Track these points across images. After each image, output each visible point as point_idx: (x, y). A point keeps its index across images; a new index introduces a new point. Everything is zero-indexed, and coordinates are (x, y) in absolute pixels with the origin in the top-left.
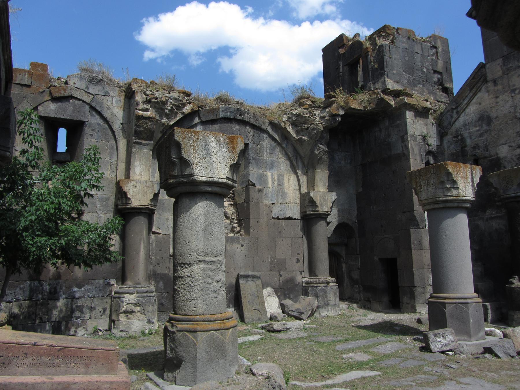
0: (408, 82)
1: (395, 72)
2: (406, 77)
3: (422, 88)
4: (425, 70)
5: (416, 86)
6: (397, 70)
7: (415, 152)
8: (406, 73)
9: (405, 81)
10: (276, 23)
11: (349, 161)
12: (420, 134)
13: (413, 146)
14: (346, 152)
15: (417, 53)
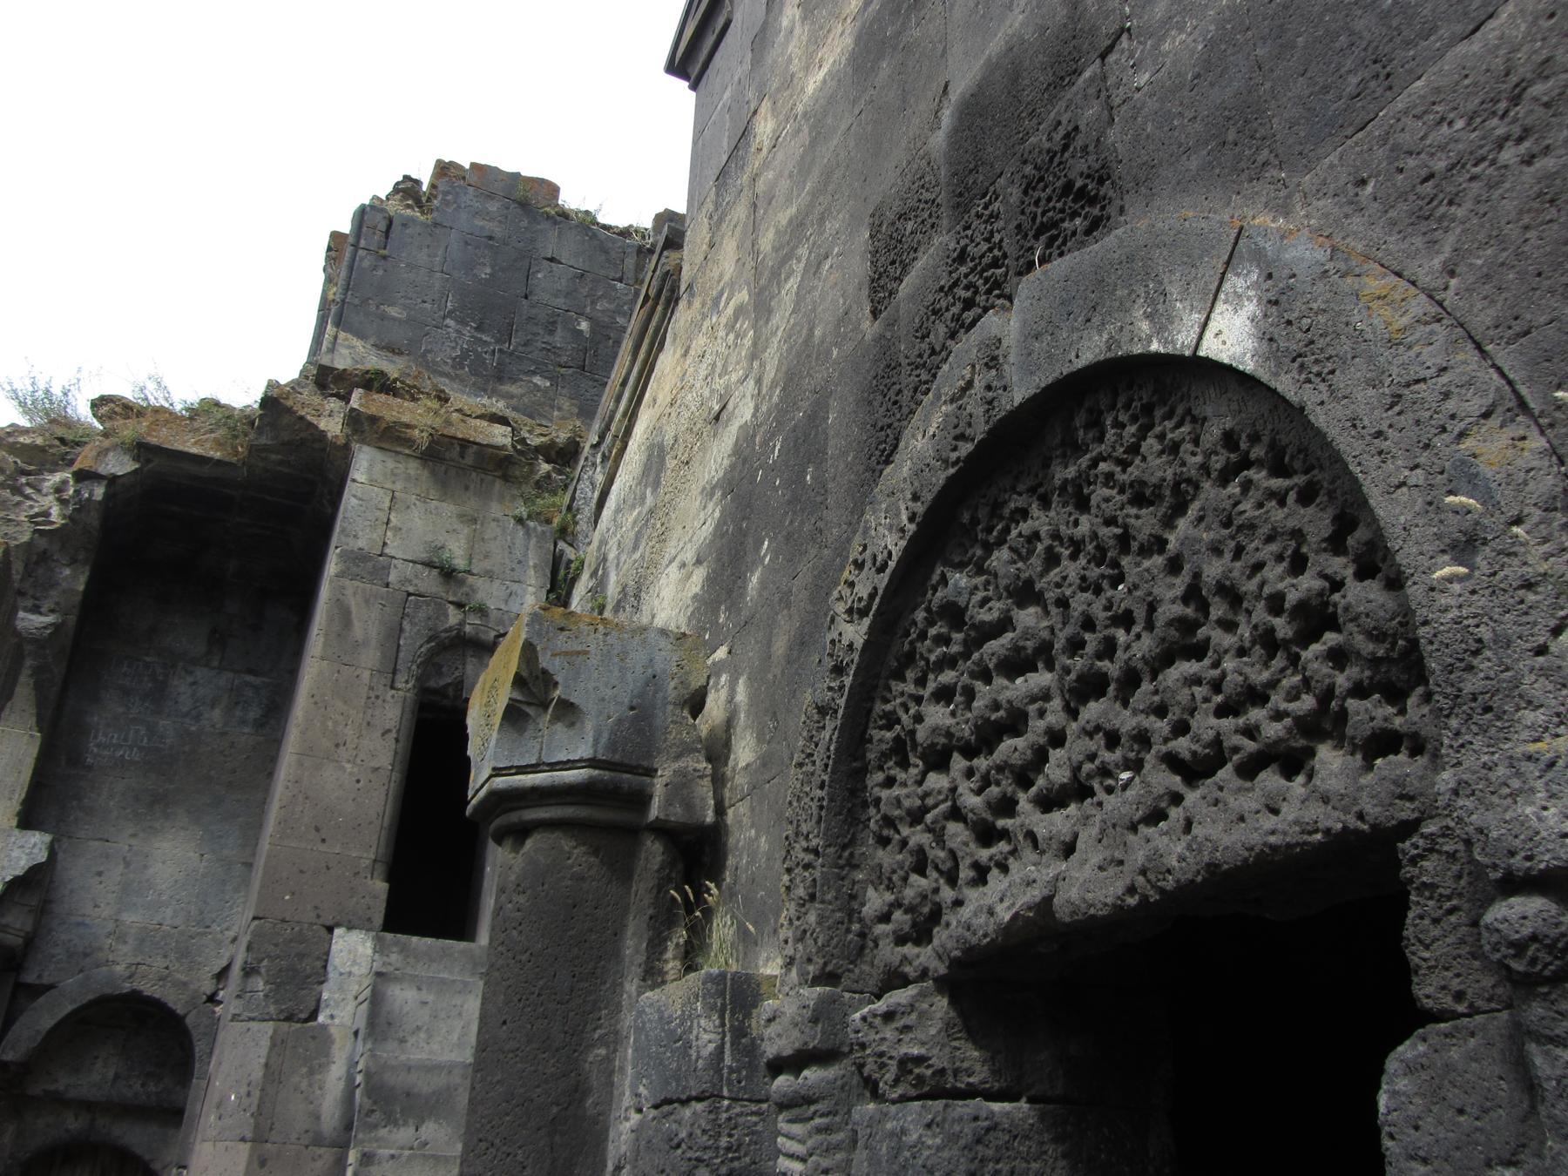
0: (465, 354)
1: (393, 311)
2: (453, 337)
3: (546, 390)
4: (584, 325)
5: (514, 380)
6: (405, 307)
7: (358, 631)
8: (462, 322)
9: (445, 354)
10: (322, 276)
11: (254, 713)
12: (424, 556)
13: (354, 604)
14: (250, 671)
15: (552, 260)
